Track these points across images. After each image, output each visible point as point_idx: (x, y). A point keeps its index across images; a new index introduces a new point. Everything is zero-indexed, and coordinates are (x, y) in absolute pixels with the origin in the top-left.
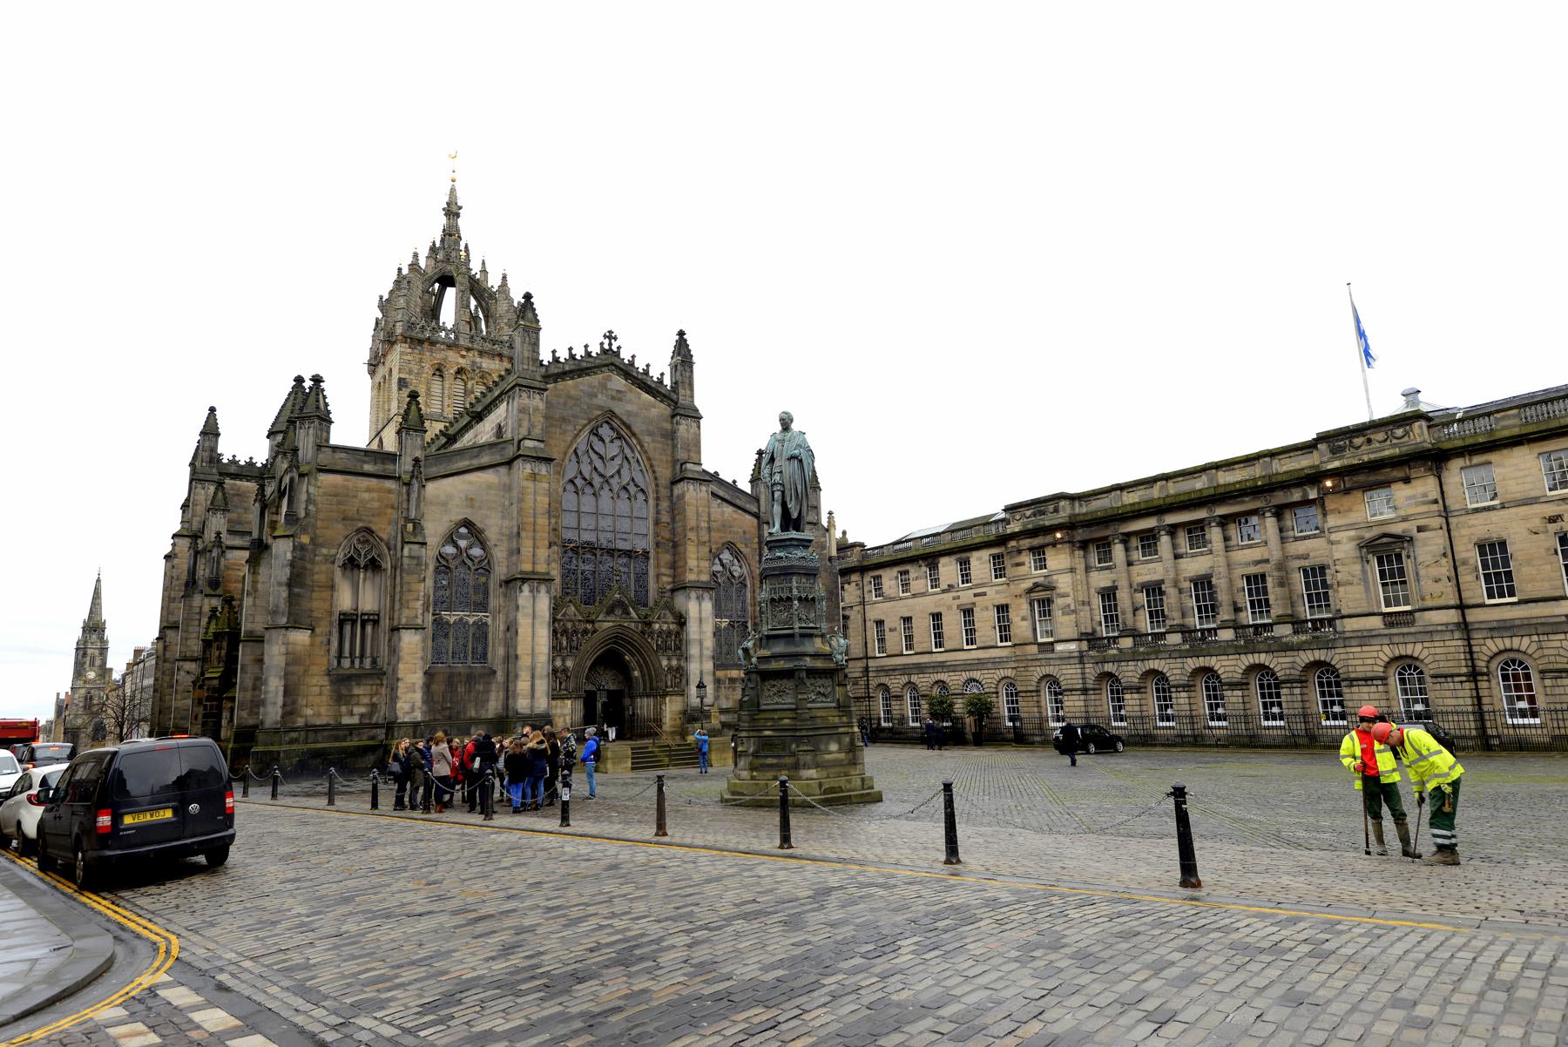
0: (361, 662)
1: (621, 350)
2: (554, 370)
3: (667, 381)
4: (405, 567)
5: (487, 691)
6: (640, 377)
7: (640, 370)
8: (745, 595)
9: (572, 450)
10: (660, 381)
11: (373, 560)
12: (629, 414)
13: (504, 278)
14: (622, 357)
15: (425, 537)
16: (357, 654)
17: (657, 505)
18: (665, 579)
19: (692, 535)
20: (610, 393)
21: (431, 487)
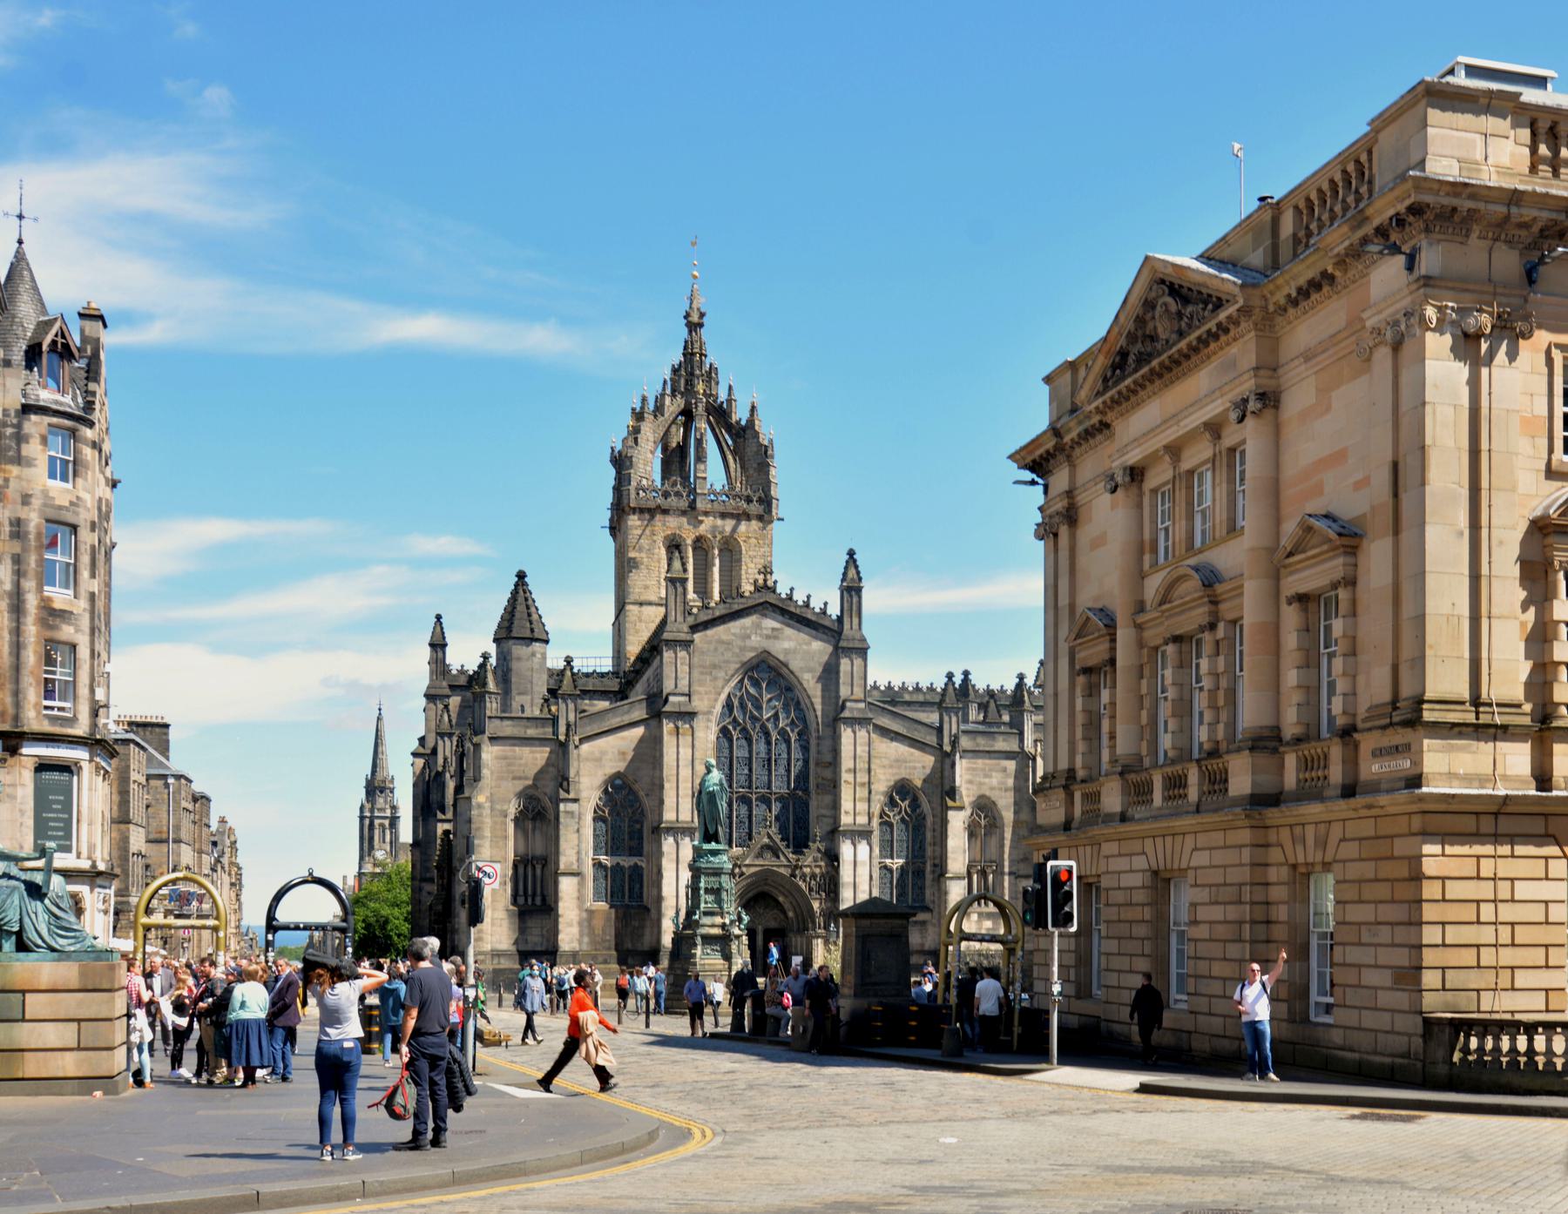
0: (533, 900)
1: (778, 585)
2: (704, 617)
3: (834, 611)
4: (562, 820)
5: (642, 927)
6: (798, 611)
7: (800, 603)
8: (924, 834)
9: (723, 696)
10: (824, 612)
11: (539, 813)
12: (787, 652)
13: (753, 408)
14: (778, 591)
15: (578, 791)
16: (530, 892)
17: (818, 745)
18: (825, 820)
19: (846, 776)
20: (765, 632)
21: (585, 747)
